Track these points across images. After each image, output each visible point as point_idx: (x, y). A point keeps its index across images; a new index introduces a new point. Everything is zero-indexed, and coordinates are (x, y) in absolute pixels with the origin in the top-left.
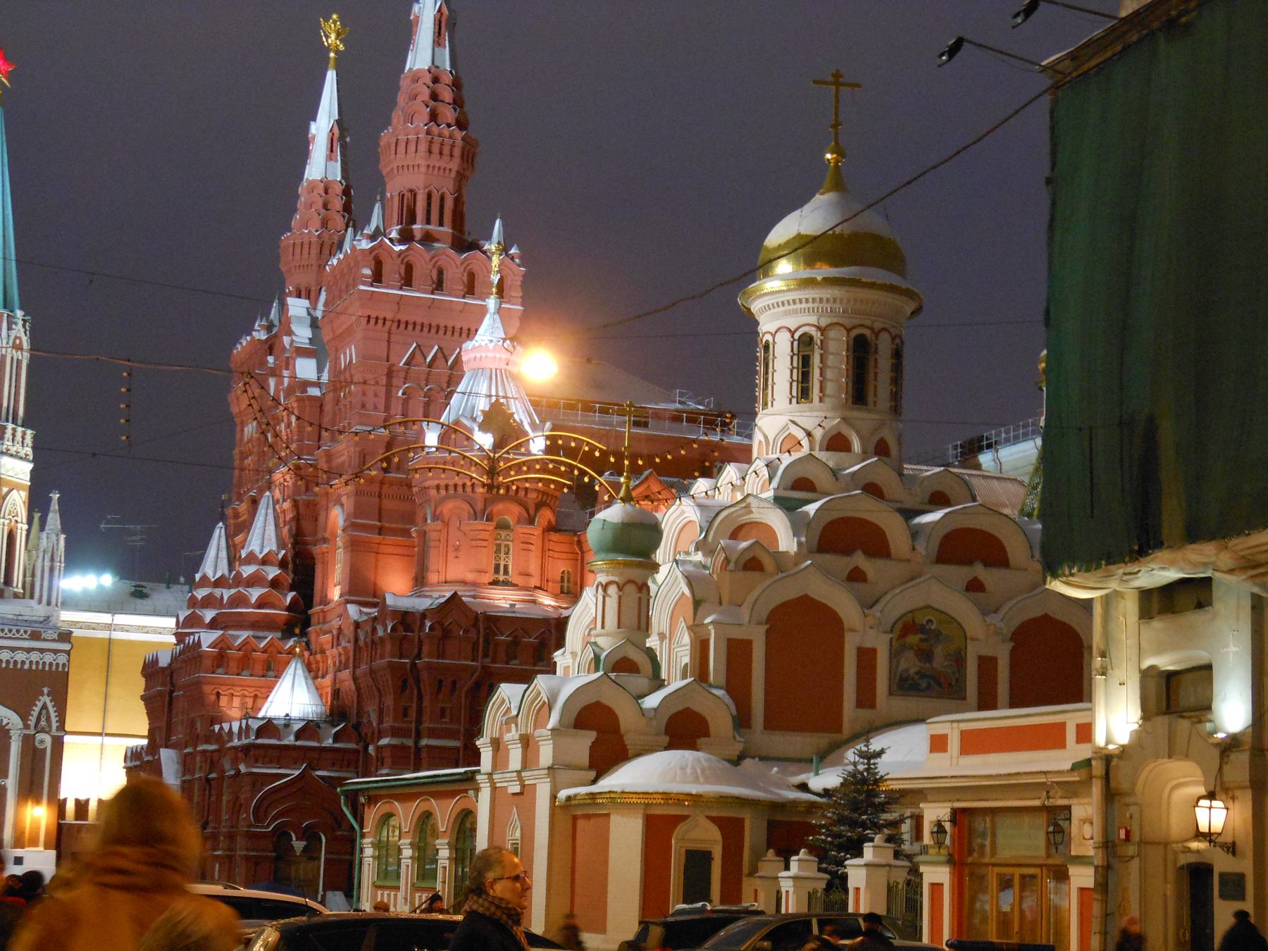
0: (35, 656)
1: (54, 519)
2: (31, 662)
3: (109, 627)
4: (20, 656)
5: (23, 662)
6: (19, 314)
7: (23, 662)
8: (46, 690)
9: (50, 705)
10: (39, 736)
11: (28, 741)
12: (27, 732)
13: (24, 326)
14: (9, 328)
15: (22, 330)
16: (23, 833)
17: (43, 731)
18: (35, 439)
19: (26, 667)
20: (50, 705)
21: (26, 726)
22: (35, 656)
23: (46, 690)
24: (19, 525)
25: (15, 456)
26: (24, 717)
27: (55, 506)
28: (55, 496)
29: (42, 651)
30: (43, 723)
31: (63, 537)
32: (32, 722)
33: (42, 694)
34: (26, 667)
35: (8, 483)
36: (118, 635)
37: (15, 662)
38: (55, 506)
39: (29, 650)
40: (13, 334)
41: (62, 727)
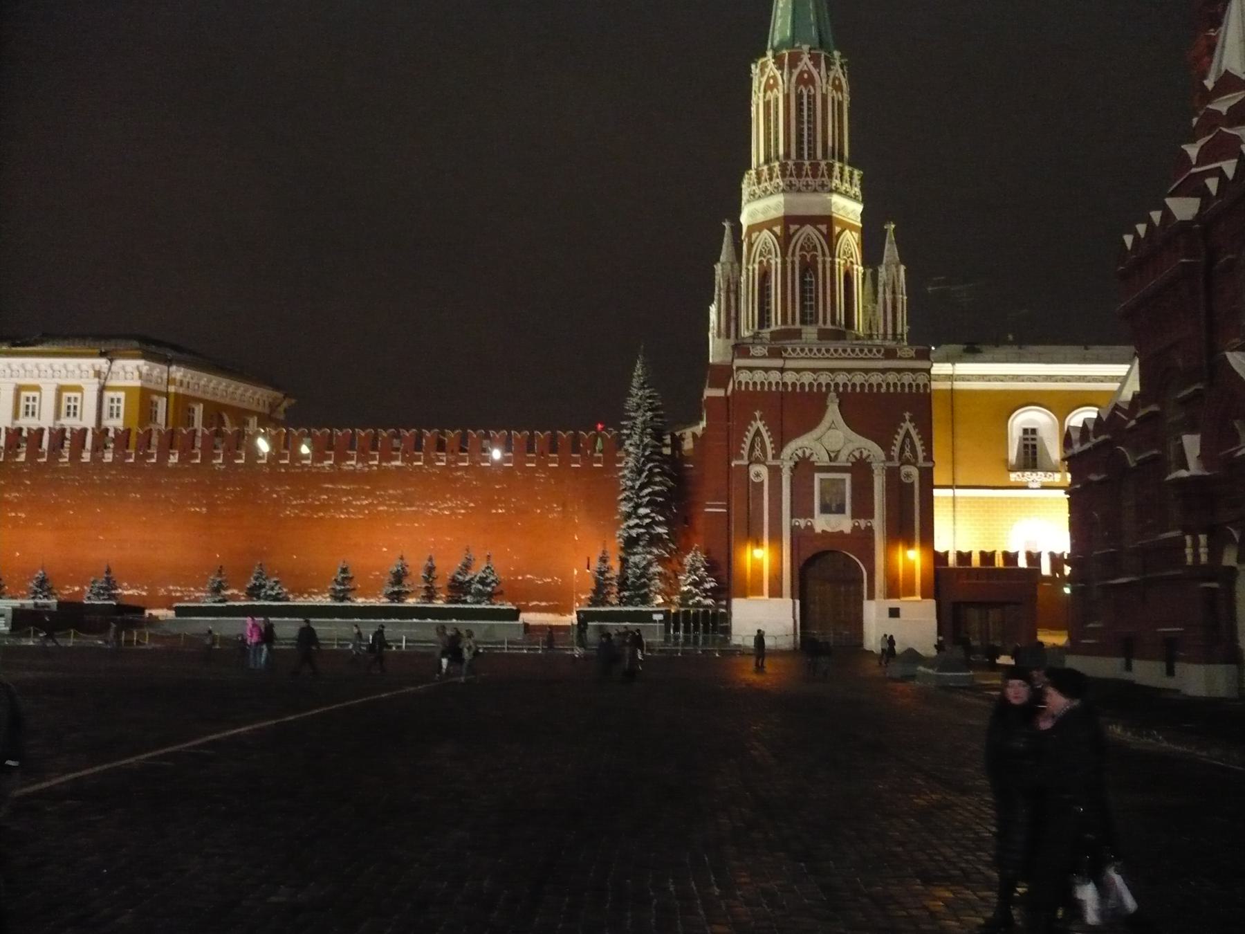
0: (892, 378)
1: (890, 251)
2: (888, 385)
3: (950, 378)
4: (875, 378)
5: (879, 385)
6: (836, 54)
7: (879, 385)
8: (907, 415)
9: (913, 433)
10: (906, 469)
12: (890, 464)
13: (842, 66)
14: (828, 69)
15: (840, 71)
17: (908, 462)
18: (862, 180)
19: (883, 390)
20: (913, 433)
21: (889, 458)
22: (892, 378)
23: (907, 415)
24: (855, 267)
25: (846, 194)
26: (886, 446)
27: (890, 237)
29: (899, 371)
30: (908, 454)
31: (902, 268)
32: (896, 450)
33: (904, 421)
34: (883, 390)
35: (840, 222)
36: (959, 385)
37: (871, 385)
38: (890, 237)
39: (884, 371)
40: (832, 74)
41: (929, 457)
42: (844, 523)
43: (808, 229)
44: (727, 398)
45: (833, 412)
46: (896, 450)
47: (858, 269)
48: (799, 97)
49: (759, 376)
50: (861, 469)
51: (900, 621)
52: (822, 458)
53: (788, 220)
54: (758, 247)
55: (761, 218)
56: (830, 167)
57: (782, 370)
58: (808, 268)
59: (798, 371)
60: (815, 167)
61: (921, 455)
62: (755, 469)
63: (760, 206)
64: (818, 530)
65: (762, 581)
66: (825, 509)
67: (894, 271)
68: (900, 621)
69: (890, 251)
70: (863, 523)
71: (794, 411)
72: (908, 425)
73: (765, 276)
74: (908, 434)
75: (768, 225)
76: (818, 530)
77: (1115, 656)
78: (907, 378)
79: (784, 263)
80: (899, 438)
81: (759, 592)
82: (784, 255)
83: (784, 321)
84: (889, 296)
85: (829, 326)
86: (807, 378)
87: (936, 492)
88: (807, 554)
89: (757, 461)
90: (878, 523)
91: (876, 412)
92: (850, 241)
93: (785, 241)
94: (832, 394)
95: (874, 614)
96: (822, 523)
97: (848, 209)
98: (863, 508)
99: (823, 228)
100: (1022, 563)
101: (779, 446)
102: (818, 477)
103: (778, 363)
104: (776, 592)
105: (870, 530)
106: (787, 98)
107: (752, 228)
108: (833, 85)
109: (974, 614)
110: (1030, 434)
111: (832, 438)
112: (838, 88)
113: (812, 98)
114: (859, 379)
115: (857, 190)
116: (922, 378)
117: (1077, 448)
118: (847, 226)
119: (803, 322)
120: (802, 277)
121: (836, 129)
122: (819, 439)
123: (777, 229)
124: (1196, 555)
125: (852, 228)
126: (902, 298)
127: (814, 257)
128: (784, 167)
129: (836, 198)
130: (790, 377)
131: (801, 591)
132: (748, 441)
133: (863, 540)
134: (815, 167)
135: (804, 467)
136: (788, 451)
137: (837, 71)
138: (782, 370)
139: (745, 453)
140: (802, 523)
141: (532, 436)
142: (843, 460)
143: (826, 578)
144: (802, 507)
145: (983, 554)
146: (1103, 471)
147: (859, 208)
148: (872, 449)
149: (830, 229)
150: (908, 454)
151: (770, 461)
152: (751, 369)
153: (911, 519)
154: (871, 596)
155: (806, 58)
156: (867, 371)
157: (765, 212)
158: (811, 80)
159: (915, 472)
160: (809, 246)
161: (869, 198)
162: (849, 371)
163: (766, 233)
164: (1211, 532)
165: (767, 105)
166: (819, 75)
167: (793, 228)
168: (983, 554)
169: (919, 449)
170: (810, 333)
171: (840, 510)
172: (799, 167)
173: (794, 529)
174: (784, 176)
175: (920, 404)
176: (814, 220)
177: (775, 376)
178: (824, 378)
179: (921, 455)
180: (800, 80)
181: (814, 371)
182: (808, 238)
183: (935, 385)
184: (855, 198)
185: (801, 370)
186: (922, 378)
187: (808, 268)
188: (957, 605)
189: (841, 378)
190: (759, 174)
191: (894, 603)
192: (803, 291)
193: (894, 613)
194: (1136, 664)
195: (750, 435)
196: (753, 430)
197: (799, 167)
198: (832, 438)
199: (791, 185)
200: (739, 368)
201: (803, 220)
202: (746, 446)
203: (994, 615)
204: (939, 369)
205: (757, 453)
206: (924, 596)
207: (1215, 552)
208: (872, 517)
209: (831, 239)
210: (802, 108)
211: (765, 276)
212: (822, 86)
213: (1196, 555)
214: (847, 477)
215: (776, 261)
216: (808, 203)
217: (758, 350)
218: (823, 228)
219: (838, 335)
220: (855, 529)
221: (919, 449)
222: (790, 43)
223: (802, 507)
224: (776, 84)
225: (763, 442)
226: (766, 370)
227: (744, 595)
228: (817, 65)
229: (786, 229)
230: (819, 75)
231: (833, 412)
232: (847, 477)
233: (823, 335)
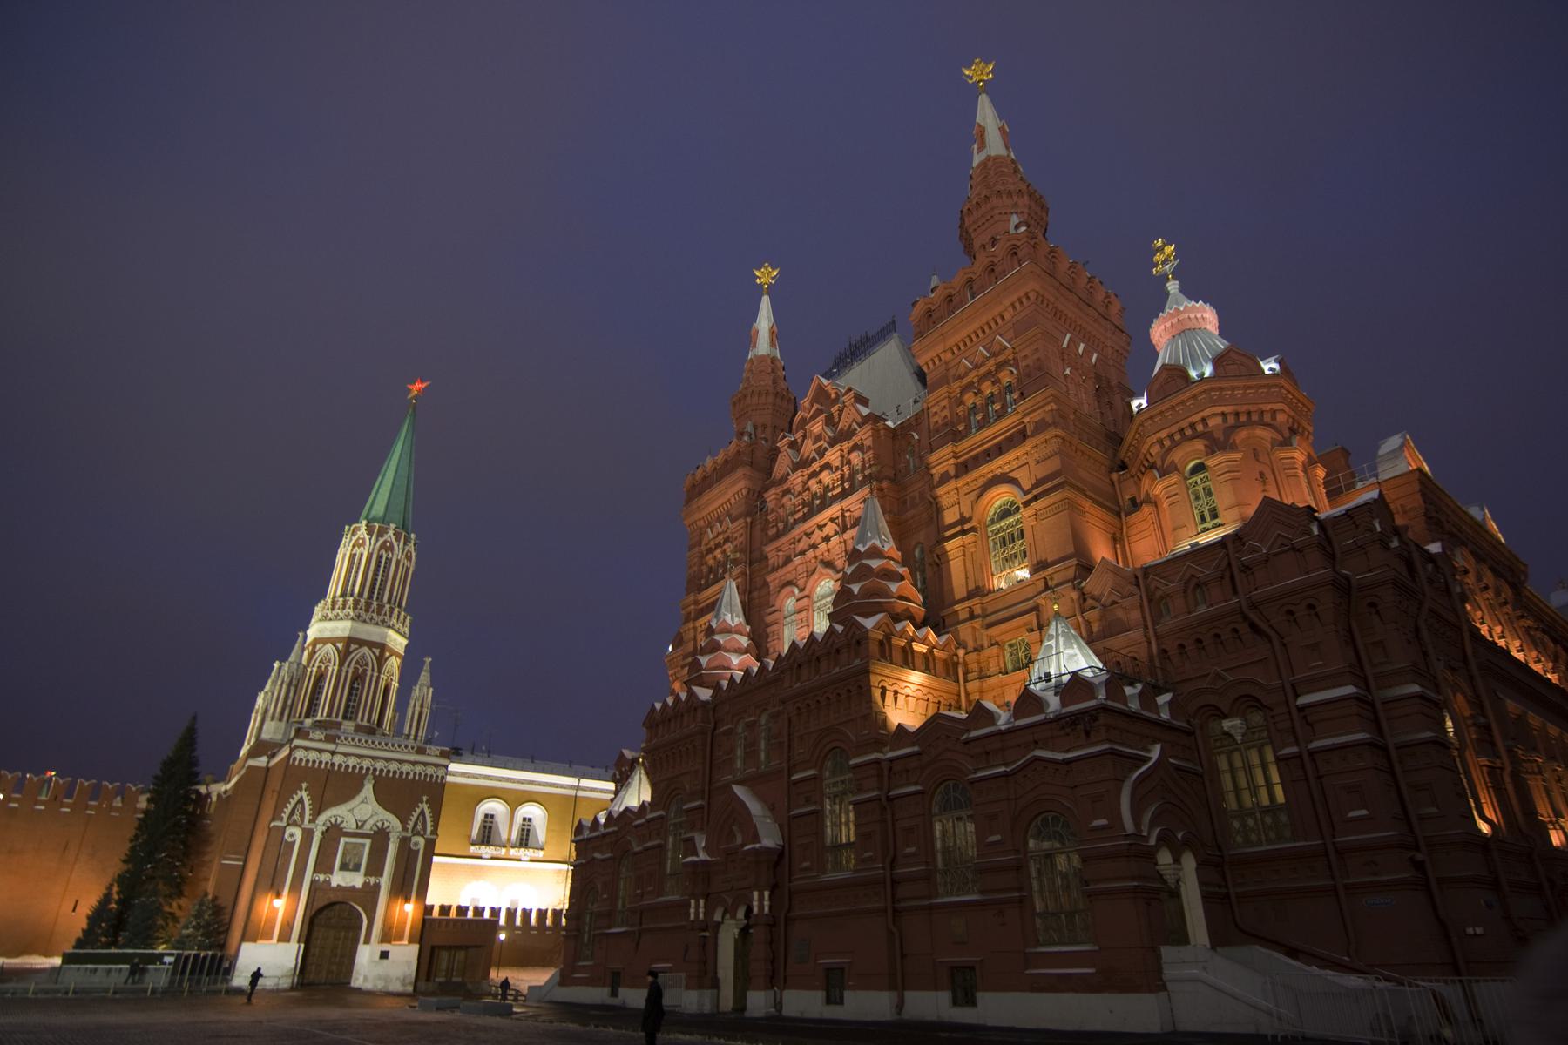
0: (419, 769)
1: (425, 677)
4: (406, 768)
9: (427, 811)
10: (415, 839)
11: (404, 842)
16: (391, 928)
17: (418, 834)
20: (427, 811)
21: (405, 829)
22: (419, 769)
25: (398, 631)
26: (404, 821)
27: (427, 667)
28: (428, 660)
29: (425, 764)
30: (419, 827)
32: (410, 827)
38: (427, 667)
39: (414, 763)
41: (435, 832)
42: (357, 880)
43: (365, 650)
44: (268, 769)
45: (368, 790)
46: (410, 827)
47: (395, 685)
48: (380, 557)
49: (312, 755)
50: (380, 837)
51: (382, 964)
52: (350, 826)
53: (350, 640)
54: (318, 656)
55: (327, 634)
56: (392, 610)
57: (333, 753)
58: (358, 678)
59: (346, 755)
60: (381, 607)
61: (429, 829)
62: (289, 830)
63: (326, 626)
64: (334, 884)
65: (273, 928)
66: (344, 867)
67: (423, 691)
68: (382, 964)
69: (425, 677)
70: (372, 880)
71: (335, 786)
72: (425, 806)
73: (321, 677)
74: (423, 813)
75: (333, 641)
76: (334, 884)
77: (880, 989)
78: (430, 771)
79: (340, 671)
80: (415, 815)
81: (267, 936)
82: (341, 665)
83: (329, 714)
84: (417, 709)
85: (365, 723)
86: (352, 761)
87: (435, 859)
88: (319, 904)
89: (295, 824)
90: (385, 881)
91: (400, 794)
92: (394, 664)
93: (344, 655)
94: (370, 777)
95: (366, 955)
96: (339, 879)
97: (397, 641)
98: (375, 868)
99: (377, 651)
100: (487, 915)
101: (317, 812)
102: (343, 840)
103: (331, 747)
104: (285, 937)
105: (377, 886)
106: (370, 556)
107: (316, 641)
108: (403, 554)
109: (445, 955)
110: (489, 817)
111: (363, 810)
112: (409, 559)
113: (389, 561)
114: (393, 766)
115: (406, 630)
116: (441, 772)
117: (586, 834)
118: (394, 653)
119: (345, 717)
120: (352, 683)
121: (399, 586)
122: (351, 810)
123: (340, 646)
124: (697, 914)
125: (397, 655)
126: (427, 711)
127: (365, 671)
128: (356, 603)
129: (391, 632)
130: (338, 759)
131: (307, 938)
132: (290, 807)
133: (370, 893)
134: (381, 607)
135: (334, 832)
136: (322, 818)
137: (411, 546)
138: (333, 753)
139: (285, 817)
140: (322, 877)
141: (73, 784)
142: (367, 829)
143: (331, 927)
144: (324, 865)
145: (492, 909)
146: (599, 853)
147: (405, 642)
148: (393, 822)
149: (382, 653)
150: (419, 827)
151: (306, 824)
152: (307, 749)
153: (411, 879)
154: (367, 941)
155: (391, 532)
156: (401, 762)
157: (332, 630)
158: (391, 548)
159: (422, 841)
160: (362, 662)
161: (412, 638)
162: (387, 760)
163: (329, 646)
164: (707, 897)
165: (353, 556)
166: (398, 547)
167: (353, 647)
168: (508, 910)
169: (429, 824)
170: (349, 726)
171: (357, 868)
172: (368, 605)
173: (313, 882)
174: (355, 608)
175: (436, 791)
176: (371, 645)
177: (326, 757)
178: (366, 763)
179: (429, 829)
180: (383, 546)
181: (359, 756)
182: (364, 656)
183: (449, 779)
184: (403, 635)
185: (348, 754)
186: (441, 772)
187: (358, 678)
188: (433, 948)
189: (379, 765)
190: (334, 603)
191: (385, 947)
192: (350, 694)
193: (384, 955)
194: (910, 995)
195: (293, 802)
196: (296, 798)
197: (368, 605)
198: (363, 810)
199: (359, 616)
200: (297, 747)
201: (362, 643)
202: (288, 811)
203: (461, 955)
204: (453, 767)
205: (296, 817)
206: (410, 942)
207: (709, 911)
208: (381, 875)
209: (381, 660)
210: (380, 565)
211: (321, 677)
212: (398, 554)
213: (697, 914)
214: (368, 842)
215: (333, 669)
216: (371, 632)
217: (318, 734)
218: (377, 651)
219: (371, 731)
220: (366, 884)
221: (429, 824)
222: (384, 520)
223: (324, 865)
224: (364, 544)
225: (303, 809)
226: (320, 751)
227: (254, 940)
228: (398, 540)
229: (347, 646)
230: (398, 547)
231: (368, 790)
232: (368, 842)
233: (358, 729)
